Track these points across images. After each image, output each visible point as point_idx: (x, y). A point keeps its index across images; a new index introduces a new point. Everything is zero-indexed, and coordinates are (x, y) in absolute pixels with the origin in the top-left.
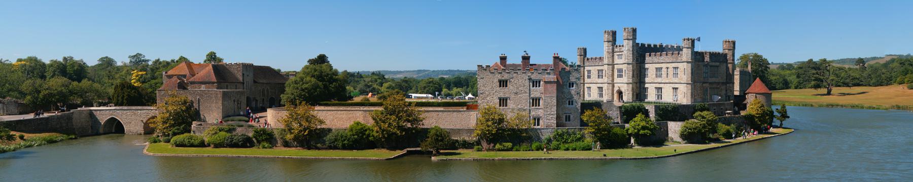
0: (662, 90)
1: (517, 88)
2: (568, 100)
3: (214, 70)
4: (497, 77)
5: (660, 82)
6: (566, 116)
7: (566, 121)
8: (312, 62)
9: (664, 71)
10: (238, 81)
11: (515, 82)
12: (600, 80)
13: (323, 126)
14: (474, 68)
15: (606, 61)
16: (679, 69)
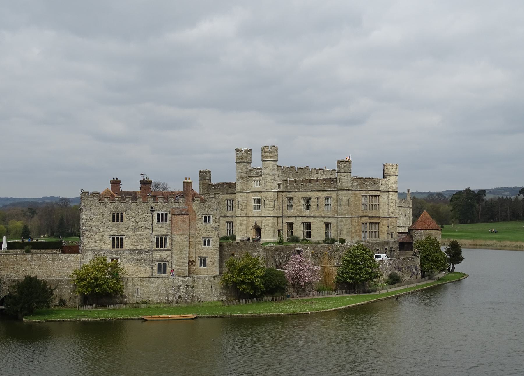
0: (311, 226)
1: (137, 223)
2: (203, 239)
5: (309, 216)
6: (201, 260)
7: (201, 265)
9: (313, 203)
11: (134, 215)
12: (230, 213)
15: (238, 187)
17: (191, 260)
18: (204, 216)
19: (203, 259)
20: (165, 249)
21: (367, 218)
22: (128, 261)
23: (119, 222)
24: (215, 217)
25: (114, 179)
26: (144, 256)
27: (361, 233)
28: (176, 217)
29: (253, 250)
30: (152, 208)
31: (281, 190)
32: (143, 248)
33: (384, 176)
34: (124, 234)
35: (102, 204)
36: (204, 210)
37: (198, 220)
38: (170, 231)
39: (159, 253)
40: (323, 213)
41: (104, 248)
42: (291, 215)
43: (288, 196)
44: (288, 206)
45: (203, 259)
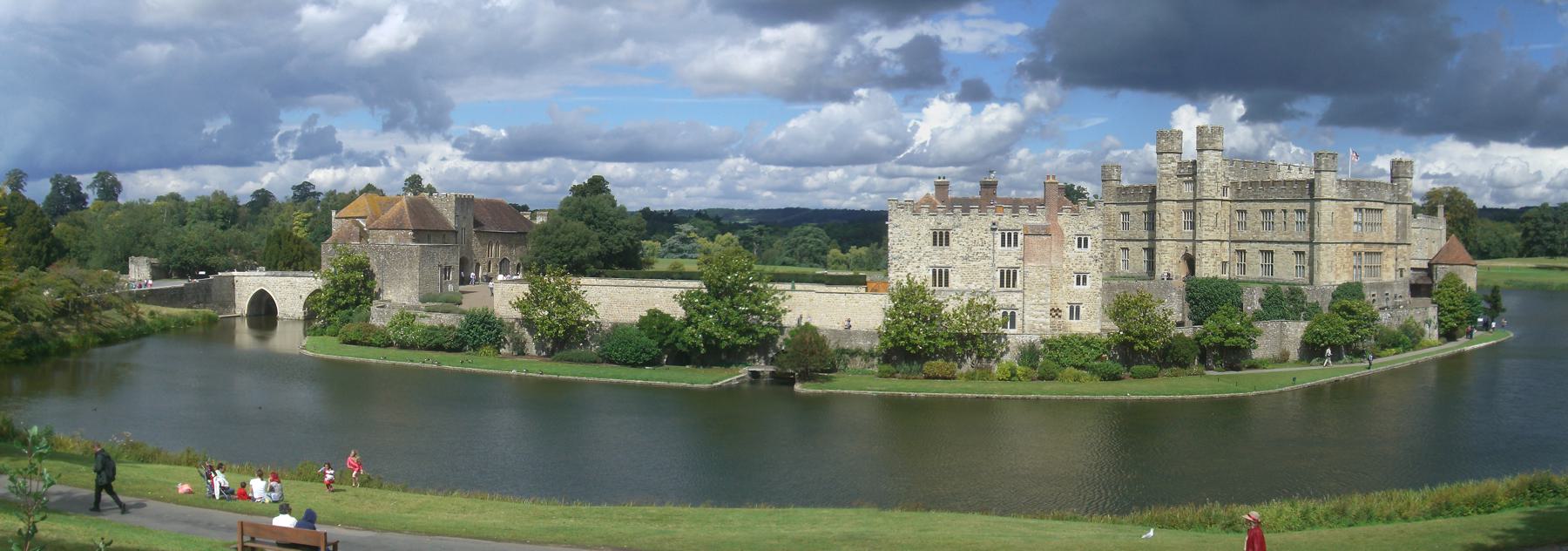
3: (409, 207)
4: (928, 225)
6: (1072, 309)
7: (1071, 318)
9: (1278, 218)
10: (448, 228)
11: (965, 235)
13: (592, 319)
18: (1077, 237)
20: (1014, 289)
21: (1362, 245)
27: (1351, 268)
28: (1031, 238)
29: (1161, 293)
30: (994, 224)
31: (1227, 198)
32: (979, 287)
33: (1392, 177)
35: (917, 217)
38: (1021, 261)
40: (1293, 236)
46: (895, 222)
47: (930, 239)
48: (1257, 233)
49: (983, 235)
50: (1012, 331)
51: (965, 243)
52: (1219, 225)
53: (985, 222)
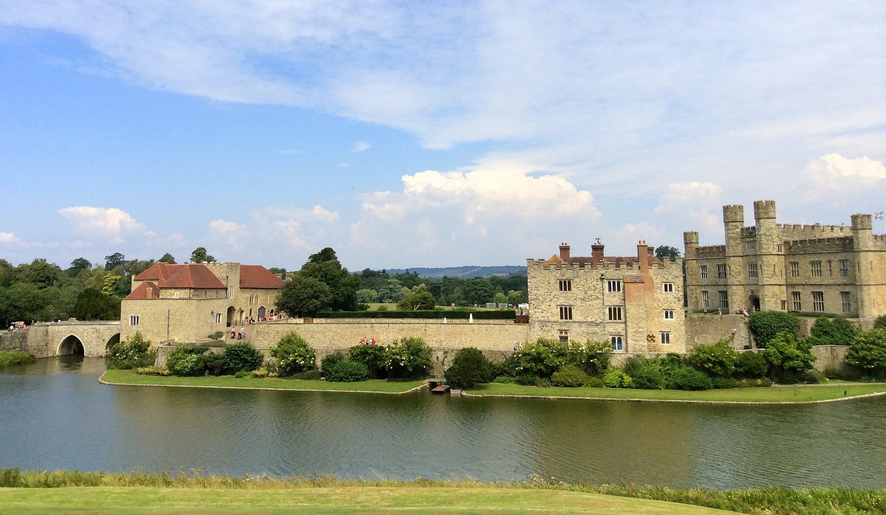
1: (586, 292)
2: (664, 311)
4: (556, 276)
7: (663, 342)
8: (315, 258)
9: (825, 266)
11: (582, 283)
14: (524, 264)
16: (848, 263)
17: (651, 335)
18: (663, 284)
19: (665, 333)
20: (619, 321)
22: (578, 334)
23: (566, 290)
24: (678, 286)
25: (563, 244)
26: (596, 328)
30: (602, 275)
32: (593, 320)
34: (573, 304)
35: (547, 271)
36: (664, 277)
37: (657, 289)
39: (612, 325)
40: (838, 280)
41: (552, 319)
42: (797, 283)
43: (792, 260)
44: (793, 271)
45: (665, 333)
46: (532, 274)
47: (558, 286)
48: (808, 278)
49: (594, 282)
50: (620, 351)
51: (582, 289)
52: (776, 273)
53: (595, 274)
